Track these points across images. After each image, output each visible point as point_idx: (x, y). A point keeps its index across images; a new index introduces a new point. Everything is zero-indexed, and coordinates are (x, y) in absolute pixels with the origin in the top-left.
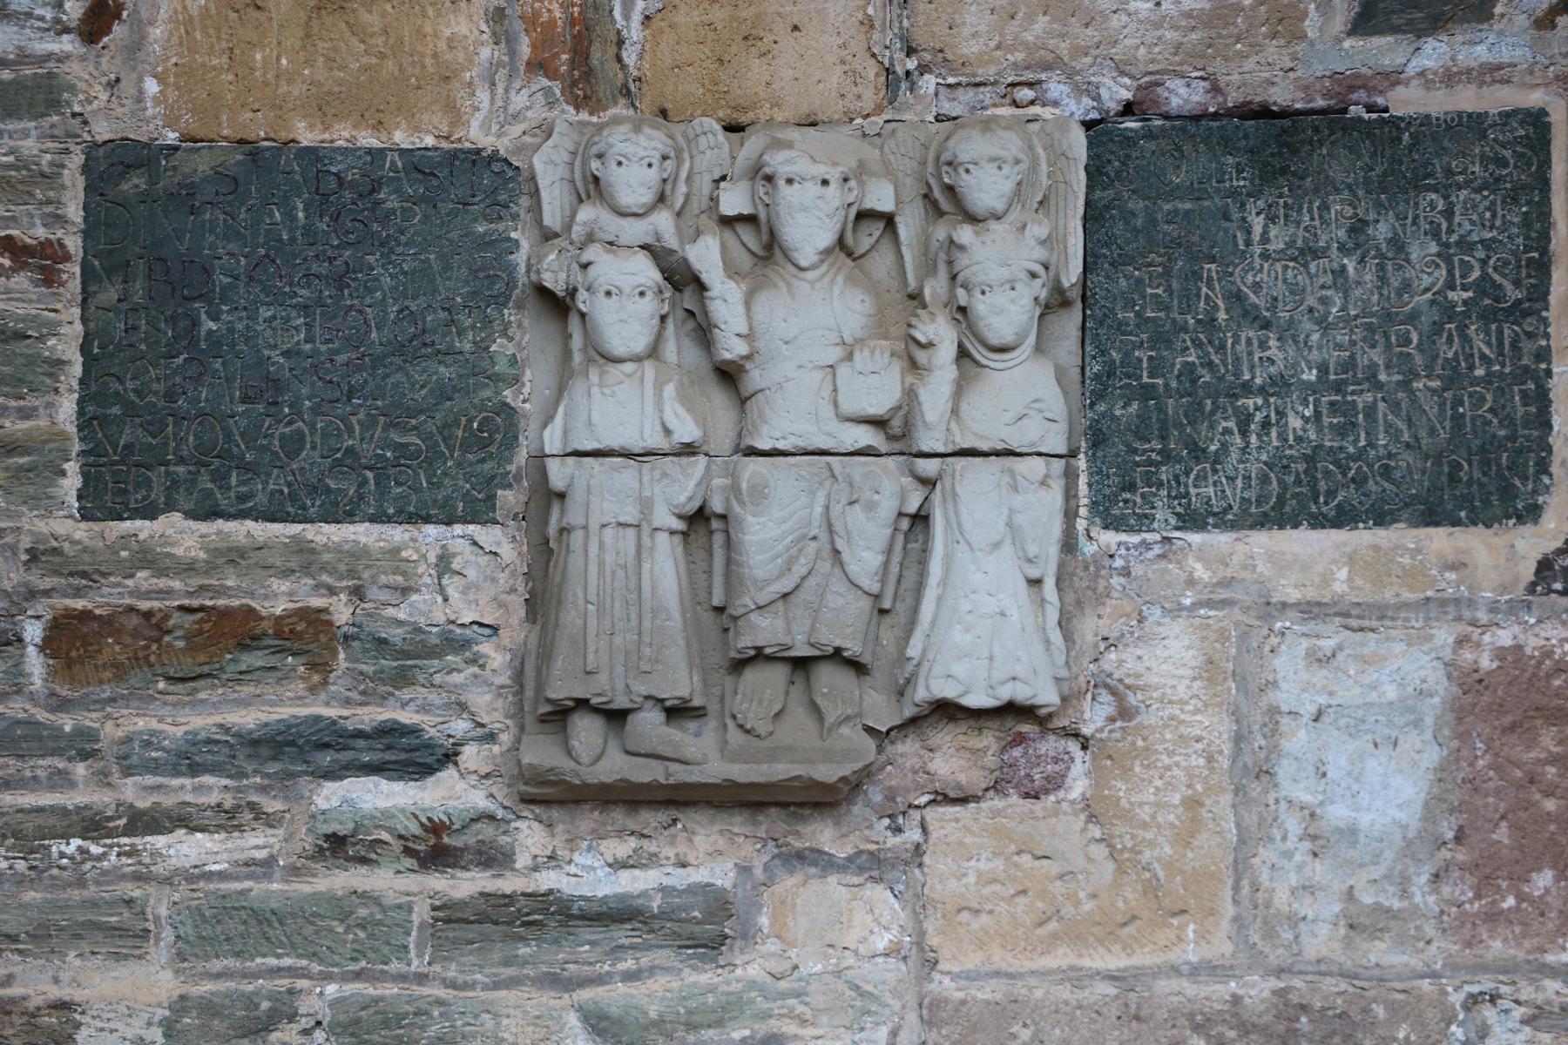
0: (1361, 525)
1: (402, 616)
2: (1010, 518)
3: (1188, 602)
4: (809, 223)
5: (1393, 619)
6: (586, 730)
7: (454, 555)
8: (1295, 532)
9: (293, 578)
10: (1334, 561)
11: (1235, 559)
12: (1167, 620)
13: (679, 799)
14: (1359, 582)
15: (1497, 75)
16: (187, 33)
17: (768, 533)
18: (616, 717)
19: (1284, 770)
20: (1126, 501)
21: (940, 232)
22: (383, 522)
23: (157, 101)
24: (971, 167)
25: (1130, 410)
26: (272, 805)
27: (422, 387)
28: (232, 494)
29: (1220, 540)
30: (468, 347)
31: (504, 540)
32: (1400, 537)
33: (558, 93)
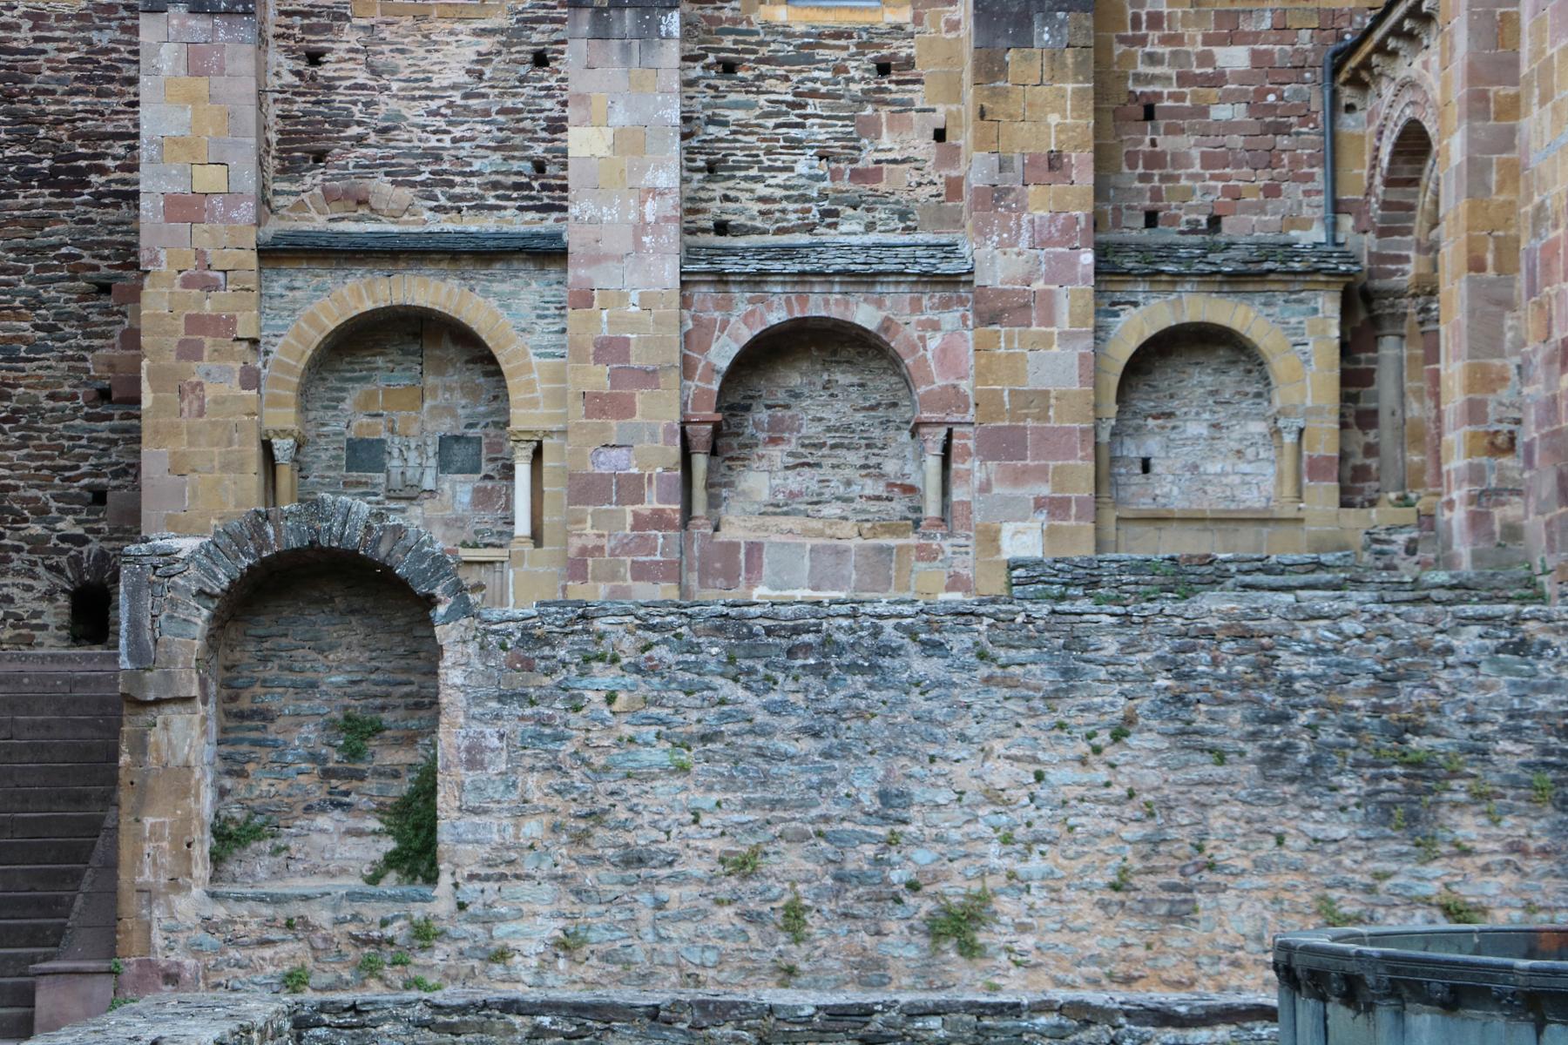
4: (413, 446)
13: (400, 498)
17: (409, 474)
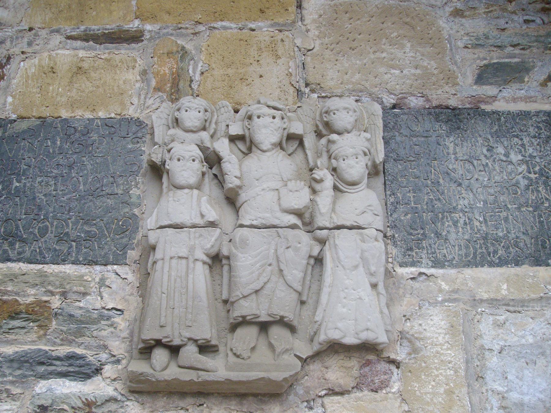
0: (509, 266)
1: (81, 305)
2: (362, 254)
3: (440, 299)
5: (527, 307)
6: (160, 356)
7: (107, 278)
8: (482, 269)
9: (37, 288)
10: (500, 281)
11: (458, 281)
12: (431, 308)
14: (512, 290)
15: (531, 100)
16: (26, 81)
17: (250, 263)
18: (174, 350)
19: (489, 376)
20: (409, 255)
21: (324, 141)
22: (77, 264)
23: (11, 104)
24: (336, 112)
25: (408, 217)
26: (15, 390)
27: (100, 208)
28: (16, 252)
29: (452, 272)
30: (120, 192)
31: (129, 272)
32: (526, 270)
33: (165, 97)
